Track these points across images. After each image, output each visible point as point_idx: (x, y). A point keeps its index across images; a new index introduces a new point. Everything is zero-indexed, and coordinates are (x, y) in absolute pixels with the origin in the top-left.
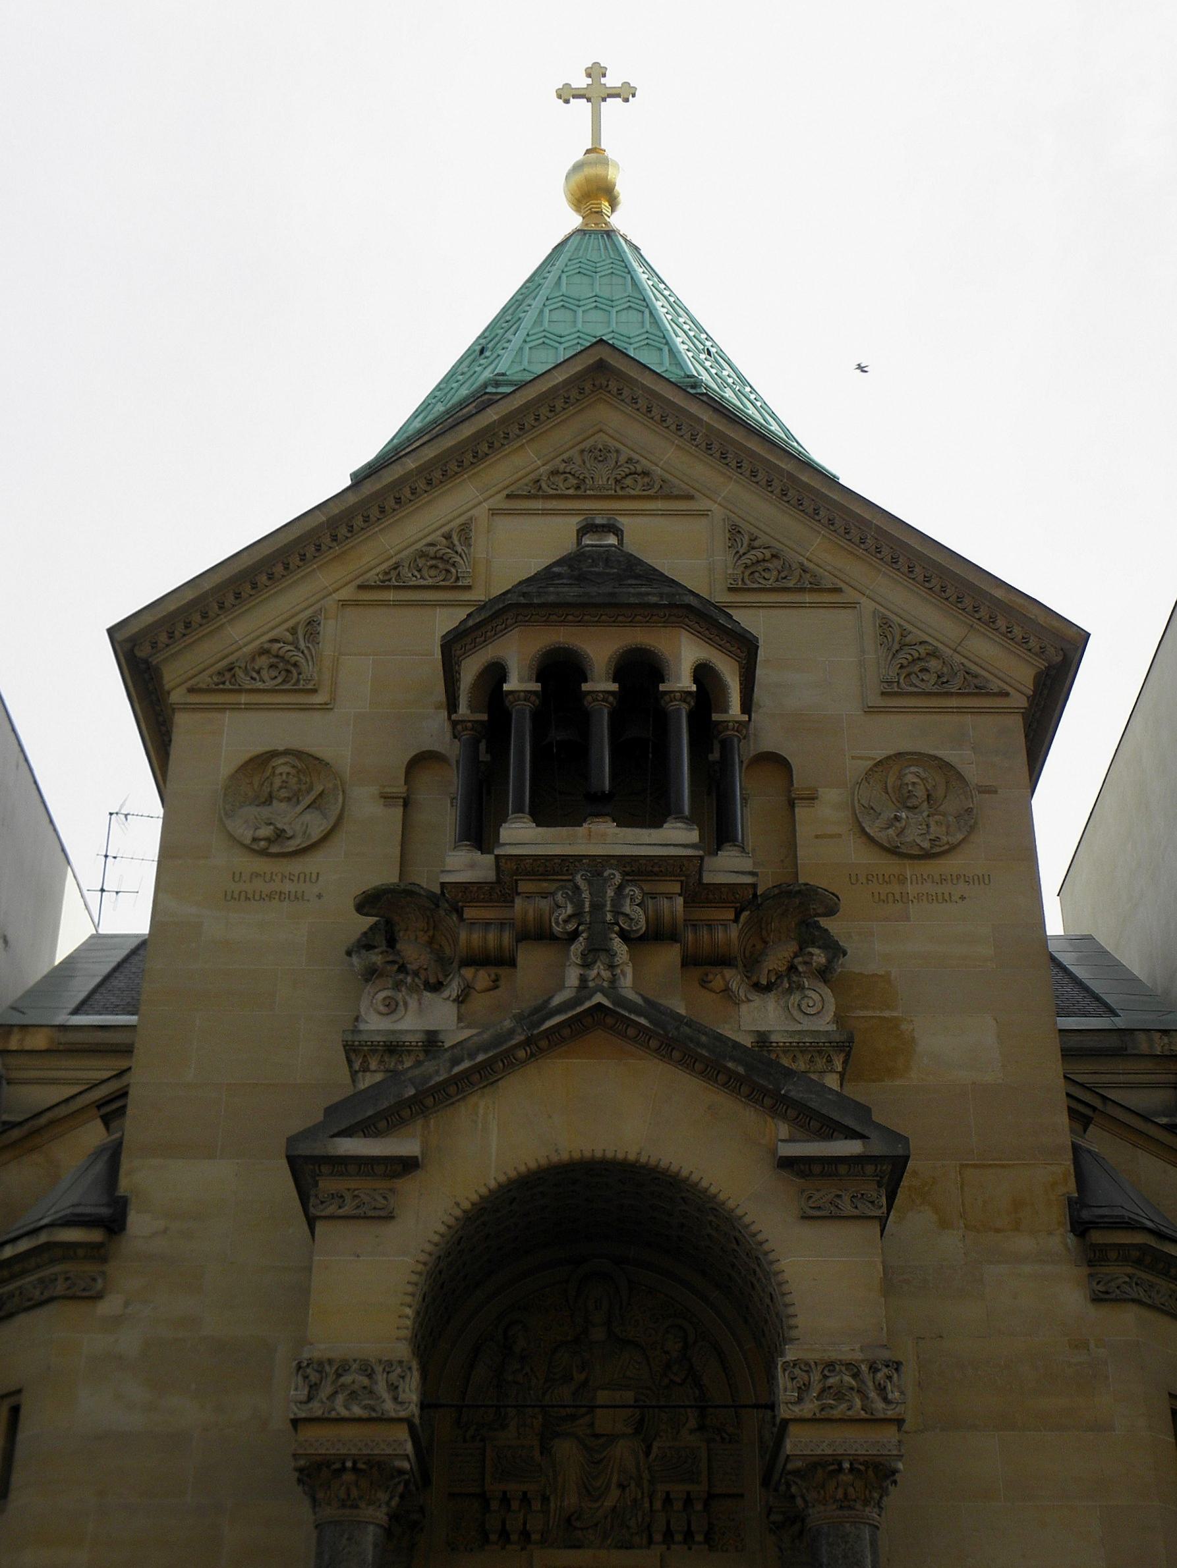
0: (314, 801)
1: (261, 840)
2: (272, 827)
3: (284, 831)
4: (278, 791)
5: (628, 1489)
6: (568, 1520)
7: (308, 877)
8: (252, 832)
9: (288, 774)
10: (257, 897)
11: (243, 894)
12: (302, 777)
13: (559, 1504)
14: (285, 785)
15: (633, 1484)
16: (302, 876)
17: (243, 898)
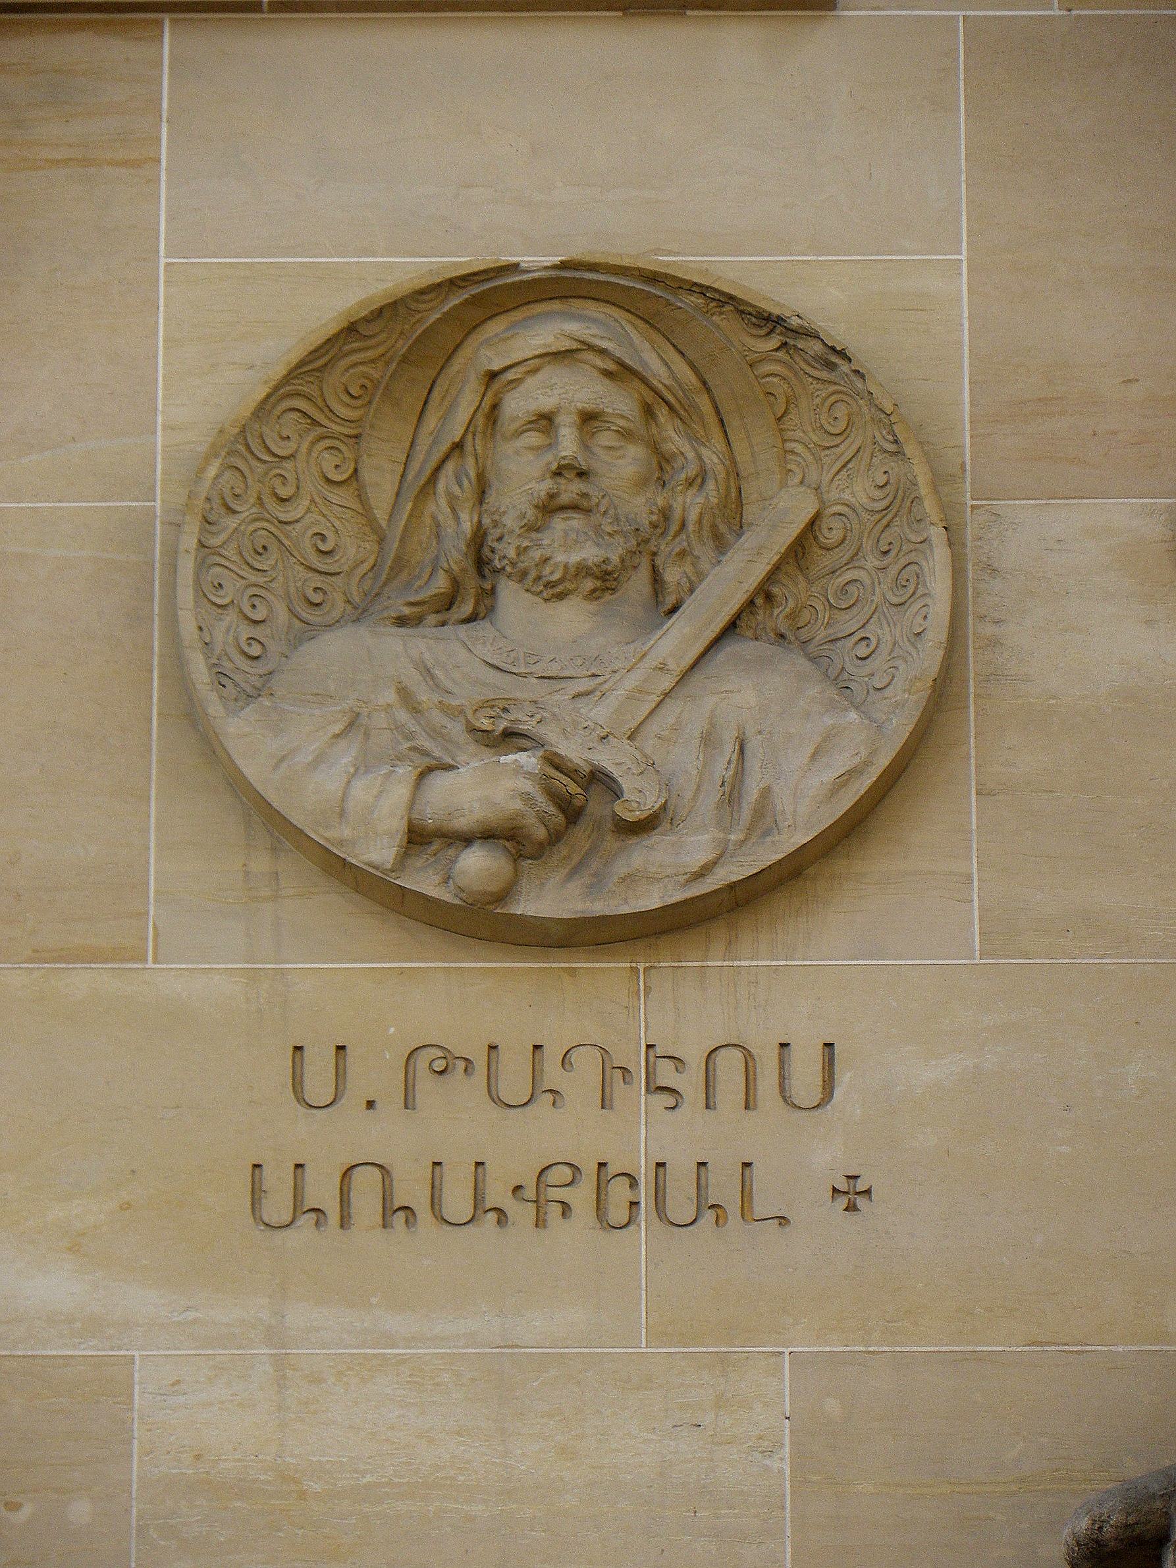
0: (764, 595)
1: (466, 840)
2: (529, 760)
3: (598, 779)
4: (532, 528)
7: (767, 1083)
8: (400, 792)
9: (589, 419)
10: (458, 1203)
11: (366, 1184)
12: (674, 439)
14: (570, 490)
16: (730, 1065)
17: (366, 1203)
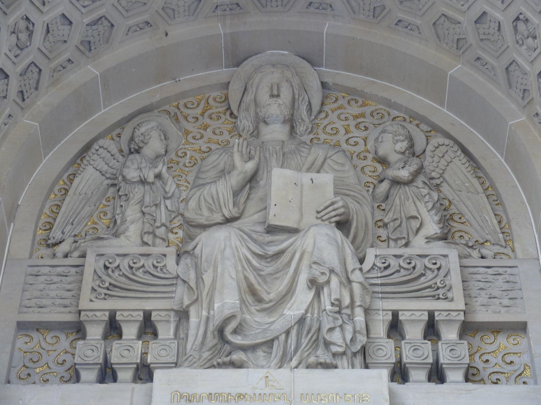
5: (326, 290)
6: (221, 331)
13: (204, 313)
15: (335, 281)
